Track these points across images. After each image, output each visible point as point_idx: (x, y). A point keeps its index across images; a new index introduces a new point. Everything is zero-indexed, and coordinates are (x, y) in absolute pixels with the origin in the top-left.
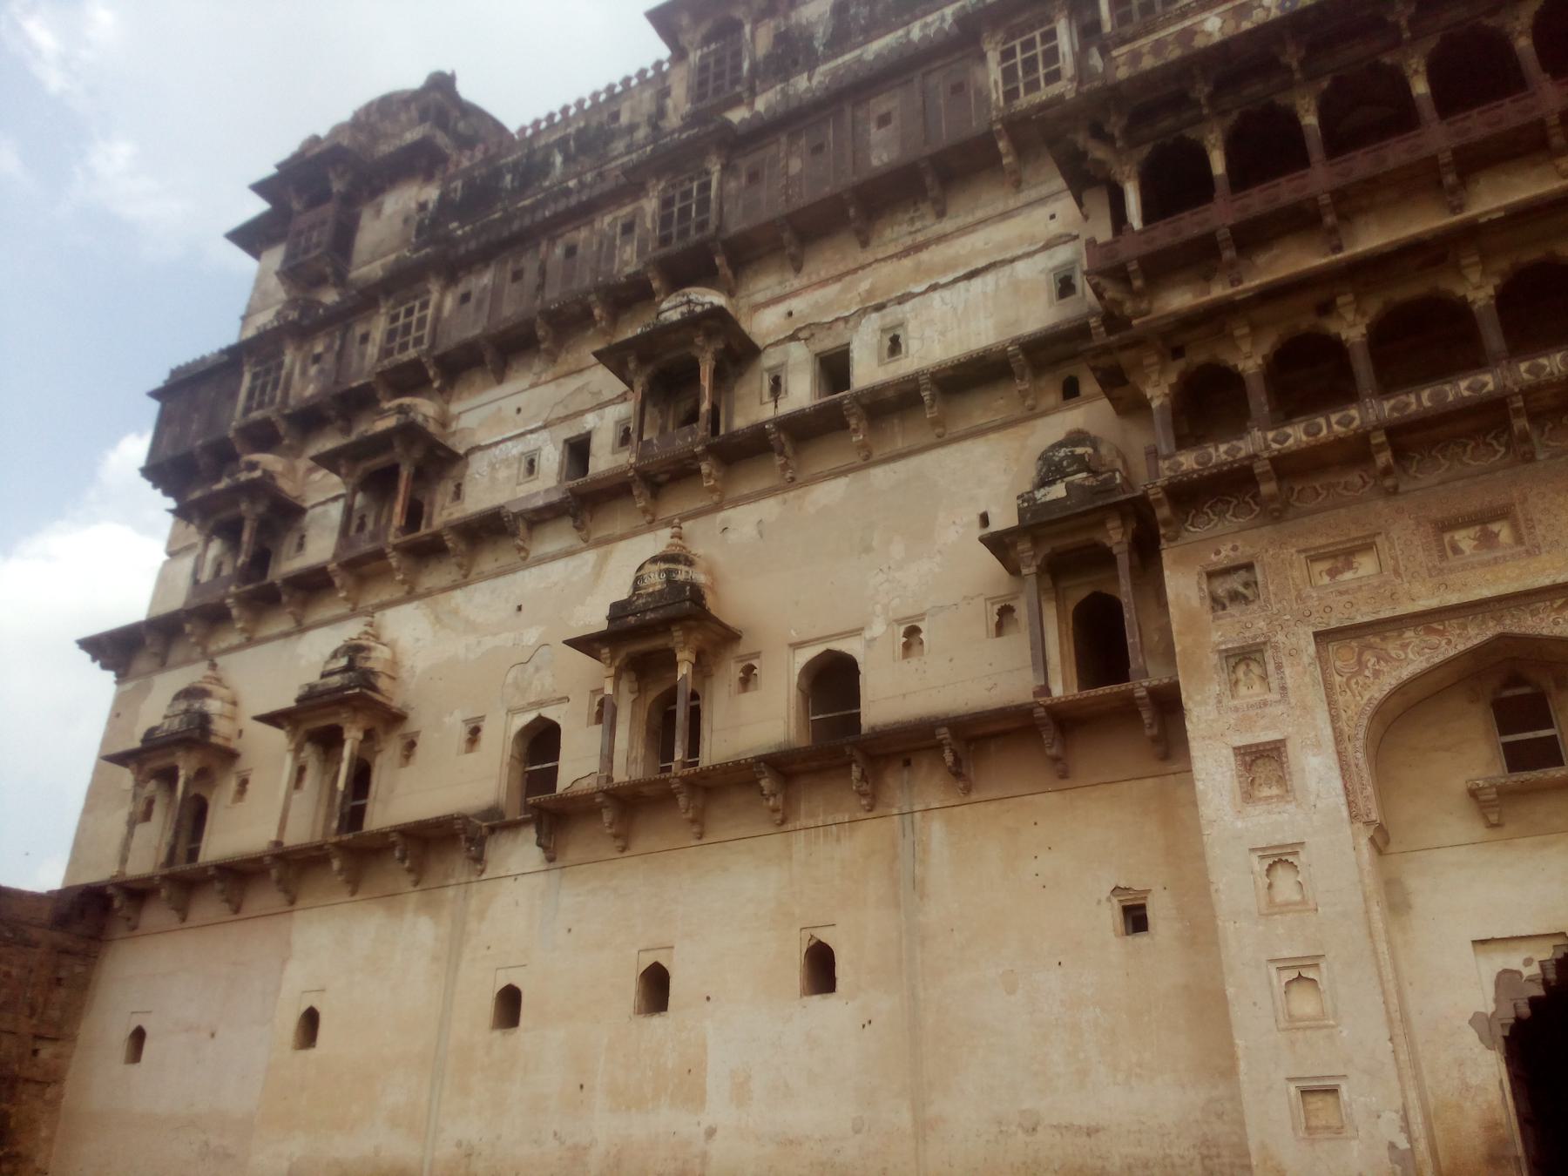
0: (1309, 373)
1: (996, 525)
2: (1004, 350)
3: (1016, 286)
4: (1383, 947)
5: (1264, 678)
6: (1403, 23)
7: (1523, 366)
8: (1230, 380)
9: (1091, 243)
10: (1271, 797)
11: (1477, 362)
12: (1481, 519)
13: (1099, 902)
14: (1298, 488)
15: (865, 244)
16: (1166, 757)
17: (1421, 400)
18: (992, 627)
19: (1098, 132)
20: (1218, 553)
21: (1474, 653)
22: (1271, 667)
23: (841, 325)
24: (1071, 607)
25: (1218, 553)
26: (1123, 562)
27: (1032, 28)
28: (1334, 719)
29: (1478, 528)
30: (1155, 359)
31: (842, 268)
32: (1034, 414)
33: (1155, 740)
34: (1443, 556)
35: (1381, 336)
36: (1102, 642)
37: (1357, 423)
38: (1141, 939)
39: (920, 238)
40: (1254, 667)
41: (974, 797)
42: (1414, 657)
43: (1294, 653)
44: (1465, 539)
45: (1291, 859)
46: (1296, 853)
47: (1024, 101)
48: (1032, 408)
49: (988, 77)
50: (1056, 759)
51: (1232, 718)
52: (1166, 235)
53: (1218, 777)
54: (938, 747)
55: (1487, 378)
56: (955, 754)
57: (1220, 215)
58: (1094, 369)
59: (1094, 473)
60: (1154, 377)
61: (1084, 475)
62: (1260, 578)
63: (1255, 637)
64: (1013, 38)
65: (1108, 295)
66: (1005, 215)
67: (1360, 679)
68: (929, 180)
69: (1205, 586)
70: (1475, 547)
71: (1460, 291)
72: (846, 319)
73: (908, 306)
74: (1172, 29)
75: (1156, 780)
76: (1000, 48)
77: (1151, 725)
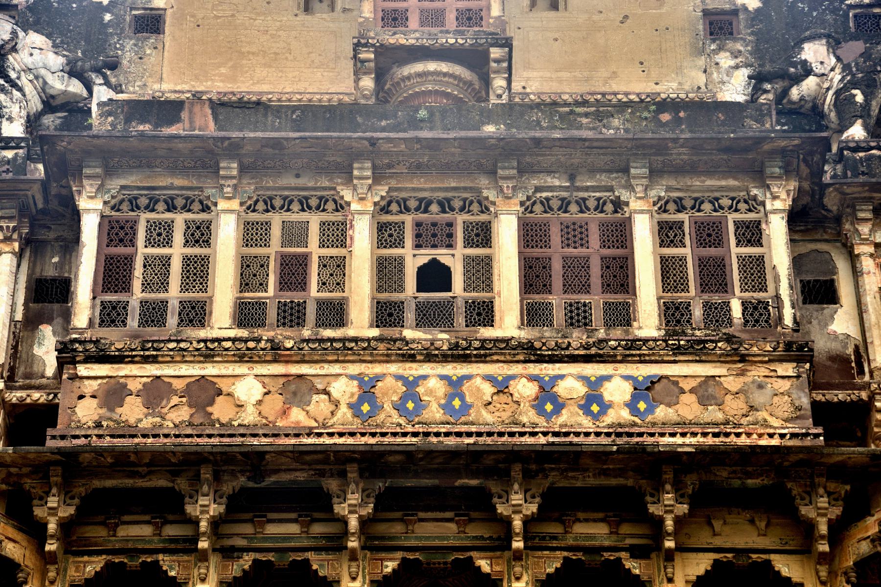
74: (185, 370)
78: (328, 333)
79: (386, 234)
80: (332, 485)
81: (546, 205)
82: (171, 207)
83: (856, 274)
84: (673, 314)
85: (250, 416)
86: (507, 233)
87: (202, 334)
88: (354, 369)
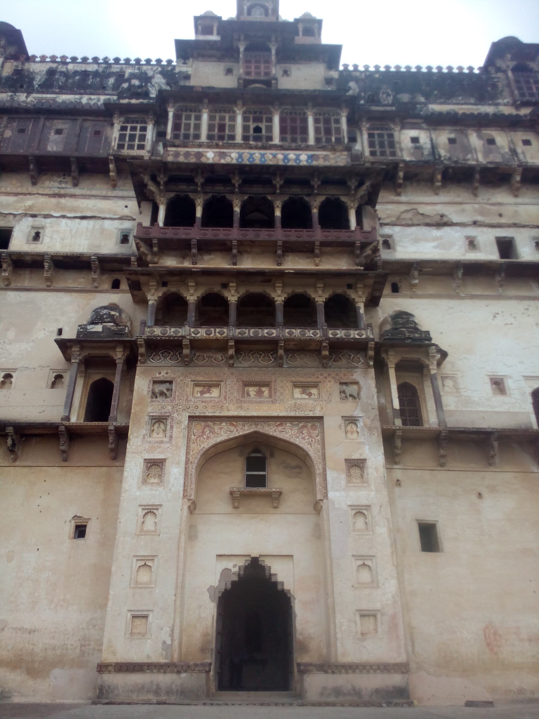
0: (213, 309)
1: (65, 336)
2: (90, 257)
3: (103, 230)
4: (182, 554)
5: (165, 431)
6: (278, 186)
7: (287, 330)
8: (182, 302)
9: (140, 224)
10: (154, 483)
11: (272, 325)
12: (260, 385)
13: (65, 522)
14: (198, 354)
15: (34, 184)
16: (114, 458)
17: (250, 333)
18: (50, 383)
19: (154, 179)
20: (160, 373)
21: (245, 436)
22: (168, 427)
23: (11, 217)
24: (91, 382)
25: (160, 373)
26: (120, 367)
27: (137, 123)
28: (187, 453)
29: (258, 388)
30: (155, 283)
31: (19, 190)
32: (96, 290)
33: (112, 450)
34: (243, 396)
35: (243, 302)
36: (100, 401)
37: (225, 335)
38: (81, 541)
39: (62, 192)
40: (162, 426)
41: (17, 463)
42: (223, 434)
43: (179, 423)
44: (252, 391)
45: (155, 511)
46: (157, 509)
47: (126, 152)
48: (96, 287)
49: (112, 133)
50: (64, 452)
51: (147, 446)
52: (172, 233)
53: (134, 471)
54: (6, 436)
55: (274, 331)
56: (13, 440)
57: (195, 233)
58: (128, 279)
59: (117, 325)
60: (153, 291)
61: (112, 324)
62: (174, 388)
63: (165, 413)
64: (128, 123)
65: (142, 249)
66: (105, 198)
67: (201, 438)
68: (73, 167)
69: (151, 387)
70: (255, 395)
71: (273, 295)
72: (15, 215)
73: (48, 220)
75: (108, 468)
76: (121, 124)
77: (112, 443)
78: (230, 142)
79: (245, 119)
80: (231, 176)
81: (286, 113)
82: (191, 111)
83: (362, 135)
84: (318, 140)
85: (211, 161)
86: (276, 120)
87: (199, 141)
88: (237, 151)
